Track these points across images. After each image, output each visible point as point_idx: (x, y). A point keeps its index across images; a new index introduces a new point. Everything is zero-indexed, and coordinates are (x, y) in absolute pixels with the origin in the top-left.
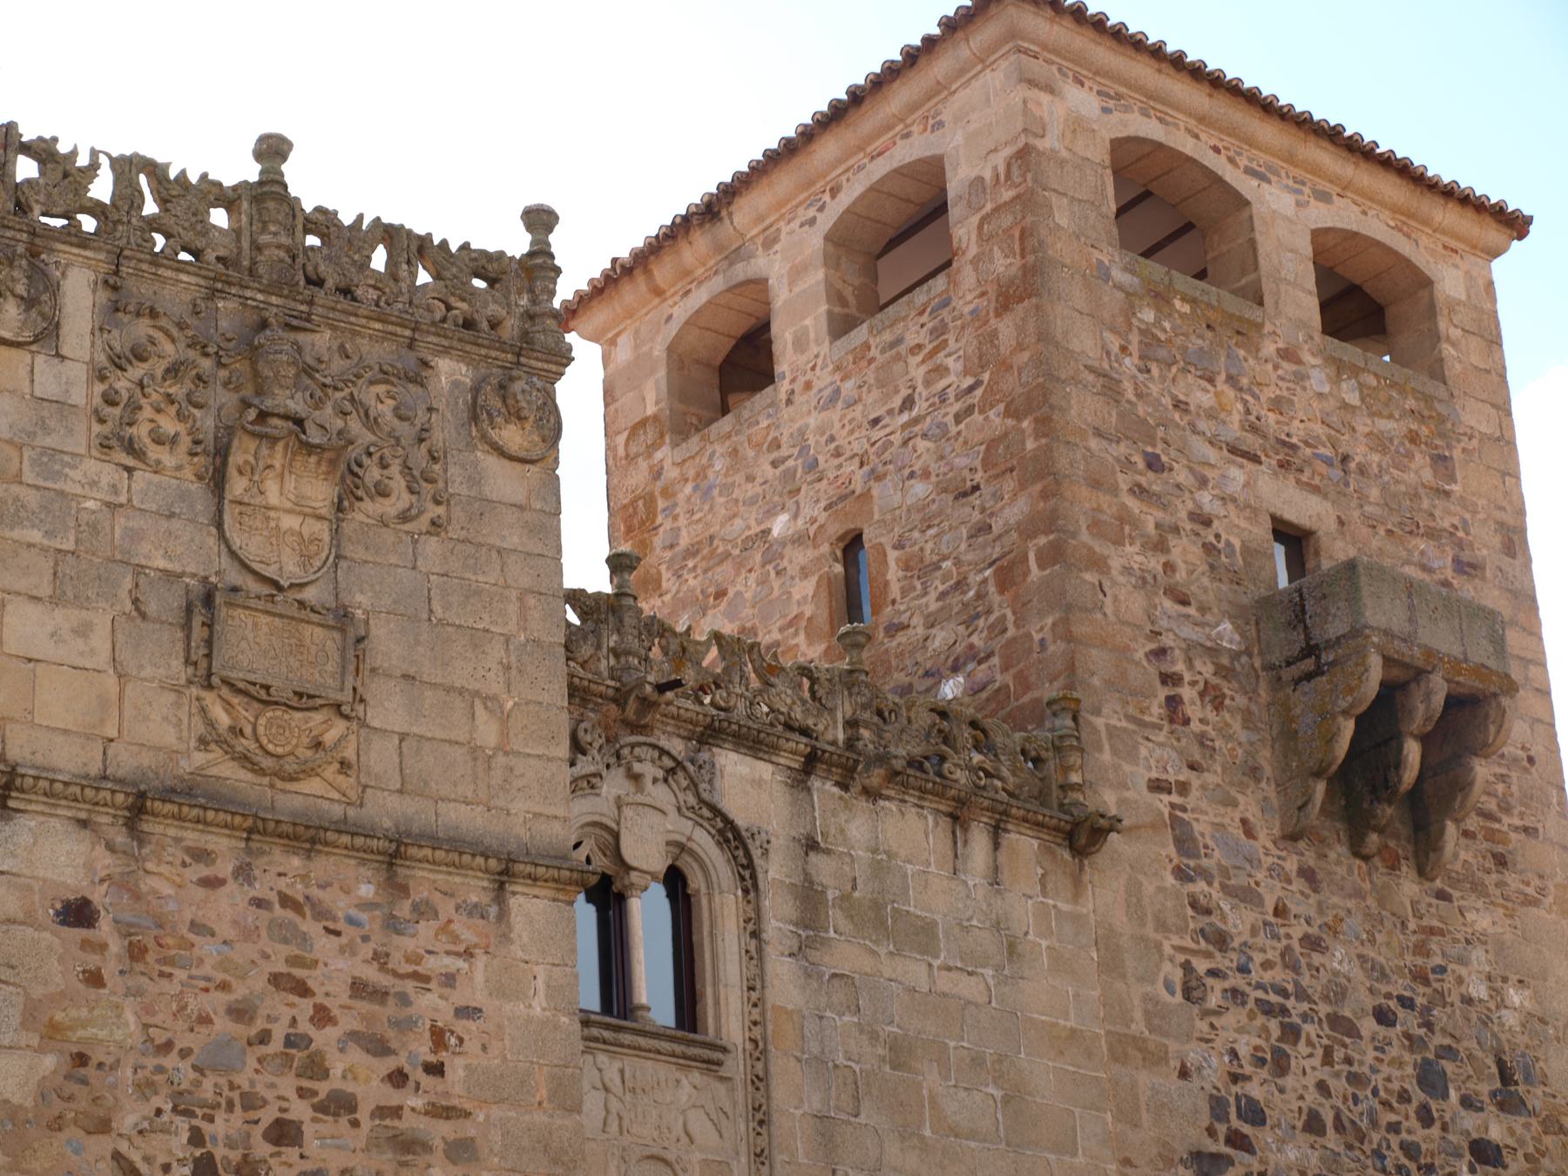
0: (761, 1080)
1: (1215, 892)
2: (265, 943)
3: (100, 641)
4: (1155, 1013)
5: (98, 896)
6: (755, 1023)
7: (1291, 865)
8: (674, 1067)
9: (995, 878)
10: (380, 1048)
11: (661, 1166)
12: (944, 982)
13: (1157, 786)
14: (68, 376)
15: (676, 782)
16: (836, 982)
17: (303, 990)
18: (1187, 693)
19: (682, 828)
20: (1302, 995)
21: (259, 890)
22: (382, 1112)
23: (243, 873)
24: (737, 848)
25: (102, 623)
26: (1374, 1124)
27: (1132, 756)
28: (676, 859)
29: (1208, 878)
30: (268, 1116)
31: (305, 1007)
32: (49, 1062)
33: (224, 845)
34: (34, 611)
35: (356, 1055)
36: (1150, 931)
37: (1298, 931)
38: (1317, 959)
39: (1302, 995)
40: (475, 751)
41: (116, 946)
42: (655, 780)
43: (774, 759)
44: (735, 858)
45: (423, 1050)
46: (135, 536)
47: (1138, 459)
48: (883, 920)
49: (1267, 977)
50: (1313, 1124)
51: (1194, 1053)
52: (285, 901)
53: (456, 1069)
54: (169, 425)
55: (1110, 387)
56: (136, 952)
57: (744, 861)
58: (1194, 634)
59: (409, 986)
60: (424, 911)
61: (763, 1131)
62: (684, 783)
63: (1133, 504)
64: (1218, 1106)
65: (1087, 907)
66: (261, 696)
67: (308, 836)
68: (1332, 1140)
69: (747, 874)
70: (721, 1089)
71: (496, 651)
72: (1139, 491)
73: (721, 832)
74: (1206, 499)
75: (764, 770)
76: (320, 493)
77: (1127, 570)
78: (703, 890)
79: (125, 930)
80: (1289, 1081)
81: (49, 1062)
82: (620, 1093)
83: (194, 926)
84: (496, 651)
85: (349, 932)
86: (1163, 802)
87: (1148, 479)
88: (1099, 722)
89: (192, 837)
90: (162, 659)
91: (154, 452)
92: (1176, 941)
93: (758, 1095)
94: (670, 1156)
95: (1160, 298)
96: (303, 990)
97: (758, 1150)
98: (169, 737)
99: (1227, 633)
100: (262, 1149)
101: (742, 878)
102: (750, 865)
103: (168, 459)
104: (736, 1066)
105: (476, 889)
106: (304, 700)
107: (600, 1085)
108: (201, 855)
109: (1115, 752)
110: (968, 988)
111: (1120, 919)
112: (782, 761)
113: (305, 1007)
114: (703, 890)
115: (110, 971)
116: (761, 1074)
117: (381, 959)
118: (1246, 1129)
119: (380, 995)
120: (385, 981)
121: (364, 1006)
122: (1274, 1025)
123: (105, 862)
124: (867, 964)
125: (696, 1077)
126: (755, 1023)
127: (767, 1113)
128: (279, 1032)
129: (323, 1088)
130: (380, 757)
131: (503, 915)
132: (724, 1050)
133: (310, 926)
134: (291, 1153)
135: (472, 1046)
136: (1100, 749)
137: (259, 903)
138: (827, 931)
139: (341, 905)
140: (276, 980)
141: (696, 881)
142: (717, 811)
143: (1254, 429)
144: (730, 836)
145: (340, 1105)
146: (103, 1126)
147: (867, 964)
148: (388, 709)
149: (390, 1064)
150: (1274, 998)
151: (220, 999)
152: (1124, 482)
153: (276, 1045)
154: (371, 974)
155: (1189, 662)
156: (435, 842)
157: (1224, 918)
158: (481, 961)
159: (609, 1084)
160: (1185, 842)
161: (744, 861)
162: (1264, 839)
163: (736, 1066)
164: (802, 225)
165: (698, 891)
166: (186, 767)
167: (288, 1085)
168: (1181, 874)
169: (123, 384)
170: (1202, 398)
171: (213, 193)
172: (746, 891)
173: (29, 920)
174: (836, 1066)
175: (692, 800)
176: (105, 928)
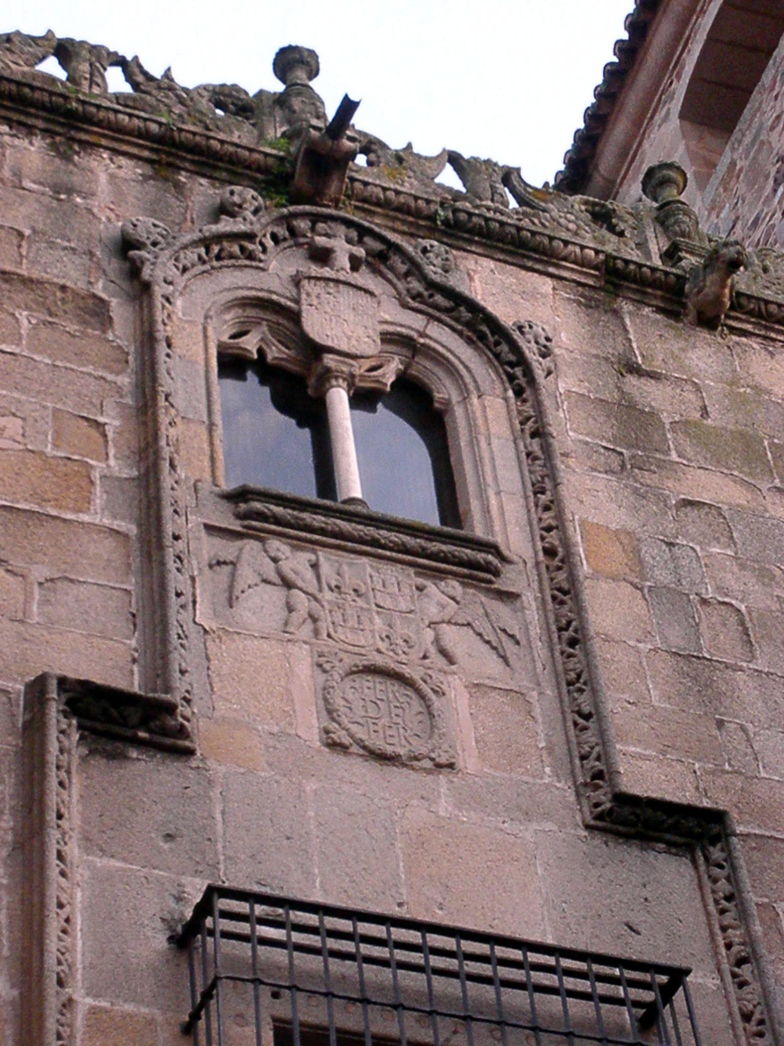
0: (565, 593)
6: (549, 529)
8: (411, 571)
11: (394, 687)
15: (392, 269)
16: (693, 513)
19: (411, 322)
24: (497, 344)
28: (408, 366)
42: (355, 262)
43: (551, 270)
44: (497, 356)
57: (512, 358)
61: (577, 651)
62: (403, 268)
69: (518, 371)
70: (501, 610)
73: (468, 324)
78: (455, 398)
82: (313, 588)
93: (566, 608)
94: (414, 672)
97: (573, 675)
101: (511, 378)
102: (522, 361)
104: (523, 577)
107: (277, 580)
112: (566, 274)
114: (455, 398)
116: (565, 586)
125: (454, 586)
126: (549, 529)
127: (582, 628)
132: (492, 548)
138: (667, 452)
141: (444, 390)
142: (459, 300)
144: (484, 328)
159: (291, 576)
161: (512, 358)
163: (523, 577)
164: (660, 126)
165: (448, 403)
172: (519, 392)
174: (704, 602)
175: (416, 285)
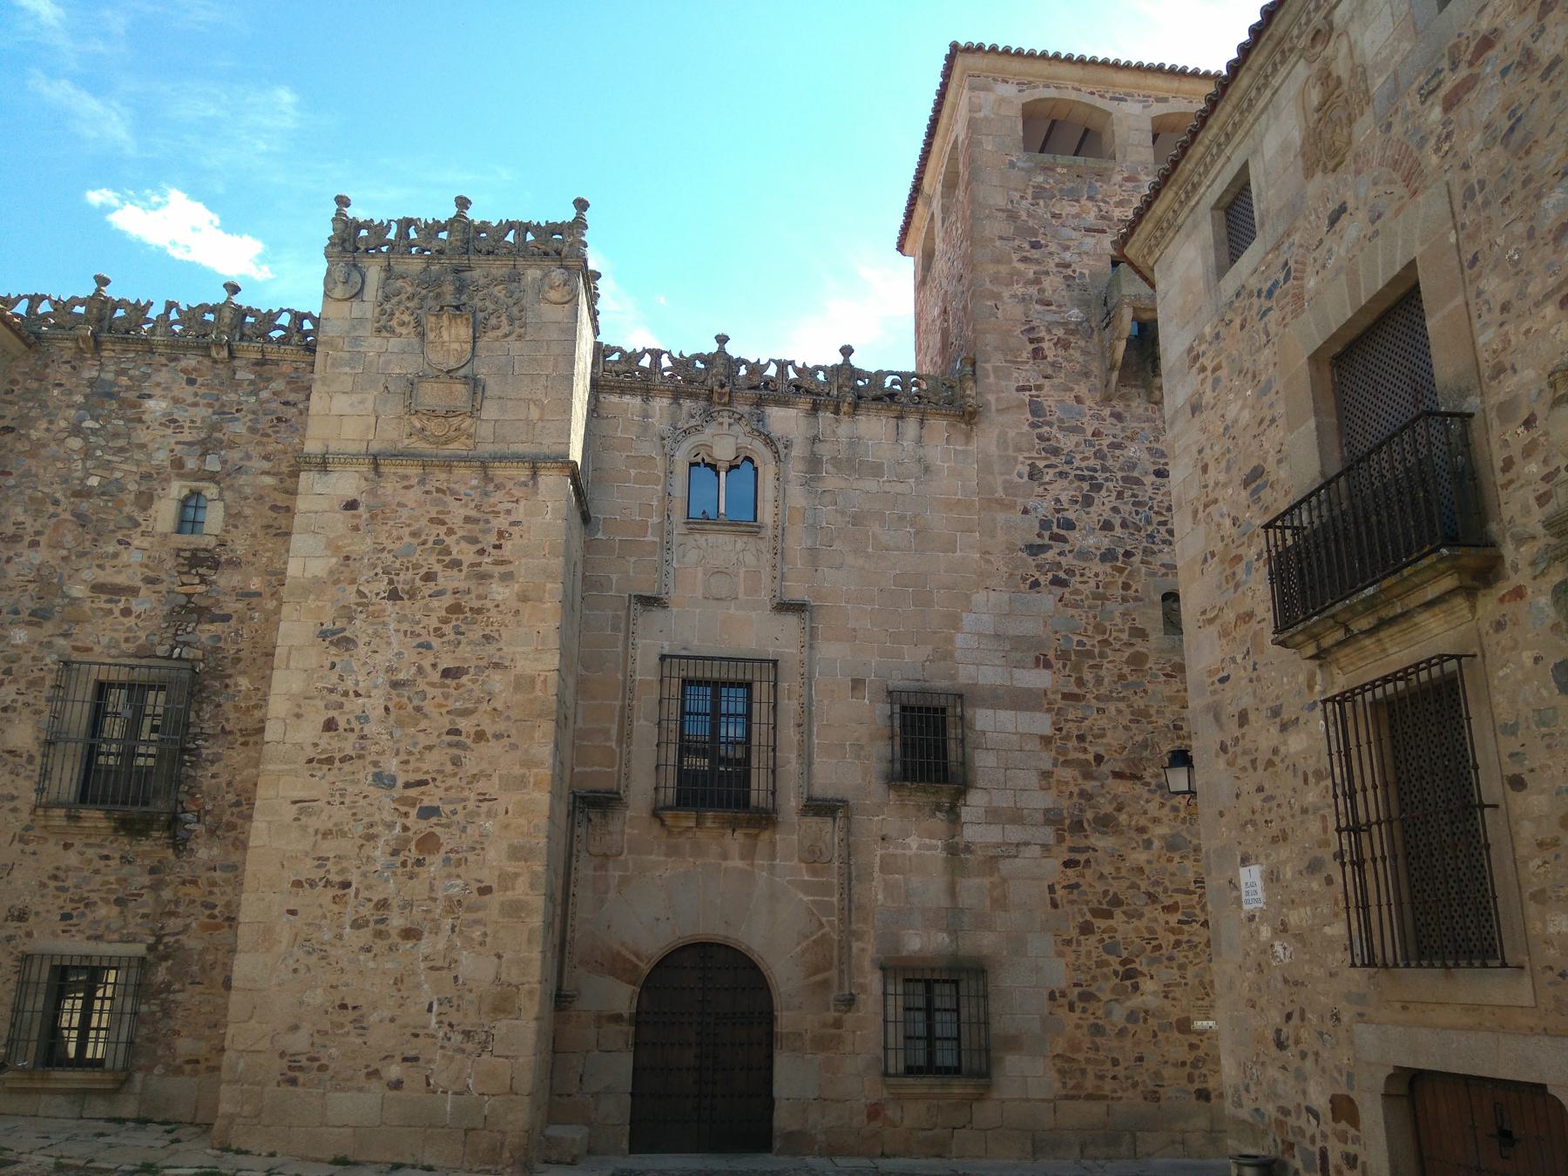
1: (1054, 430)
2: (428, 507)
3: (369, 405)
4: (1009, 487)
5: (362, 499)
7: (1107, 412)
9: (919, 441)
10: (473, 540)
12: (887, 487)
13: (1021, 389)
14: (367, 308)
17: (443, 523)
18: (1045, 345)
19: (745, 441)
20: (1105, 469)
21: (428, 488)
22: (472, 565)
23: (422, 482)
25: (370, 397)
26: (1149, 522)
27: (1008, 377)
29: (1050, 424)
30: (423, 571)
31: (444, 529)
32: (334, 560)
33: (414, 471)
34: (344, 398)
35: (463, 544)
36: (1010, 452)
37: (1106, 442)
38: (1117, 452)
39: (1105, 469)
40: (528, 422)
41: (366, 516)
45: (493, 539)
46: (388, 362)
47: (1026, 246)
48: (852, 464)
49: (1084, 464)
50: (1107, 526)
51: (1031, 504)
52: (438, 490)
53: (508, 546)
54: (406, 318)
55: (1012, 216)
56: (373, 517)
58: (1057, 317)
59: (490, 517)
60: (497, 487)
63: (1021, 266)
64: (1045, 524)
65: (973, 447)
66: (432, 413)
67: (448, 464)
68: (1118, 531)
71: (543, 381)
72: (1024, 260)
74: (1067, 256)
75: (792, 412)
76: (464, 332)
77: (1015, 296)
79: (370, 509)
80: (1092, 509)
81: (334, 560)
83: (399, 504)
84: (543, 381)
85: (465, 499)
86: (1026, 396)
87: (1035, 254)
88: (988, 366)
89: (401, 471)
90: (394, 407)
91: (398, 330)
92: (1027, 455)
95: (1047, 169)
96: (443, 523)
98: (395, 435)
99: (1075, 314)
100: (418, 583)
103: (404, 331)
105: (523, 474)
106: (450, 413)
108: (406, 477)
109: (997, 377)
110: (899, 488)
111: (993, 449)
113: (444, 529)
115: (362, 523)
117: (478, 507)
118: (1062, 532)
119: (477, 521)
120: (478, 515)
121: (469, 526)
122: (1086, 486)
123: (364, 484)
124: (843, 484)
125: (745, 539)
128: (431, 539)
129: (447, 559)
130: (485, 430)
131: (535, 484)
133: (449, 499)
134: (432, 584)
135: (516, 536)
136: (988, 377)
137: (427, 492)
139: (462, 489)
140: (431, 520)
143: (1103, 218)
145: (456, 564)
146: (353, 581)
147: (843, 484)
148: (490, 411)
149: (479, 546)
150: (1086, 473)
151: (407, 530)
152: (1015, 257)
153: (430, 544)
154: (473, 513)
155: (1049, 331)
156: (501, 458)
157: (1058, 440)
158: (523, 502)
160: (1036, 409)
162: (1089, 403)
166: (400, 446)
167: (433, 559)
168: (1033, 425)
169: (387, 307)
170: (1068, 208)
171: (438, 227)
173: (332, 510)
176: (361, 509)
